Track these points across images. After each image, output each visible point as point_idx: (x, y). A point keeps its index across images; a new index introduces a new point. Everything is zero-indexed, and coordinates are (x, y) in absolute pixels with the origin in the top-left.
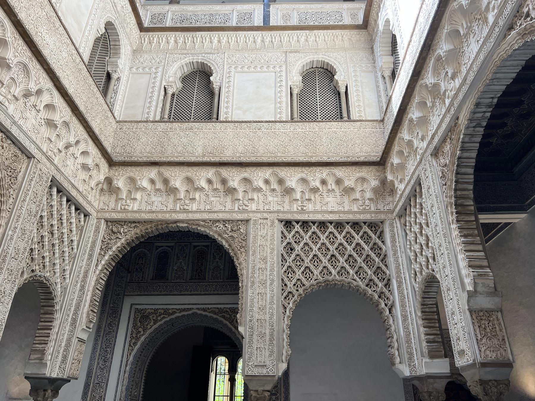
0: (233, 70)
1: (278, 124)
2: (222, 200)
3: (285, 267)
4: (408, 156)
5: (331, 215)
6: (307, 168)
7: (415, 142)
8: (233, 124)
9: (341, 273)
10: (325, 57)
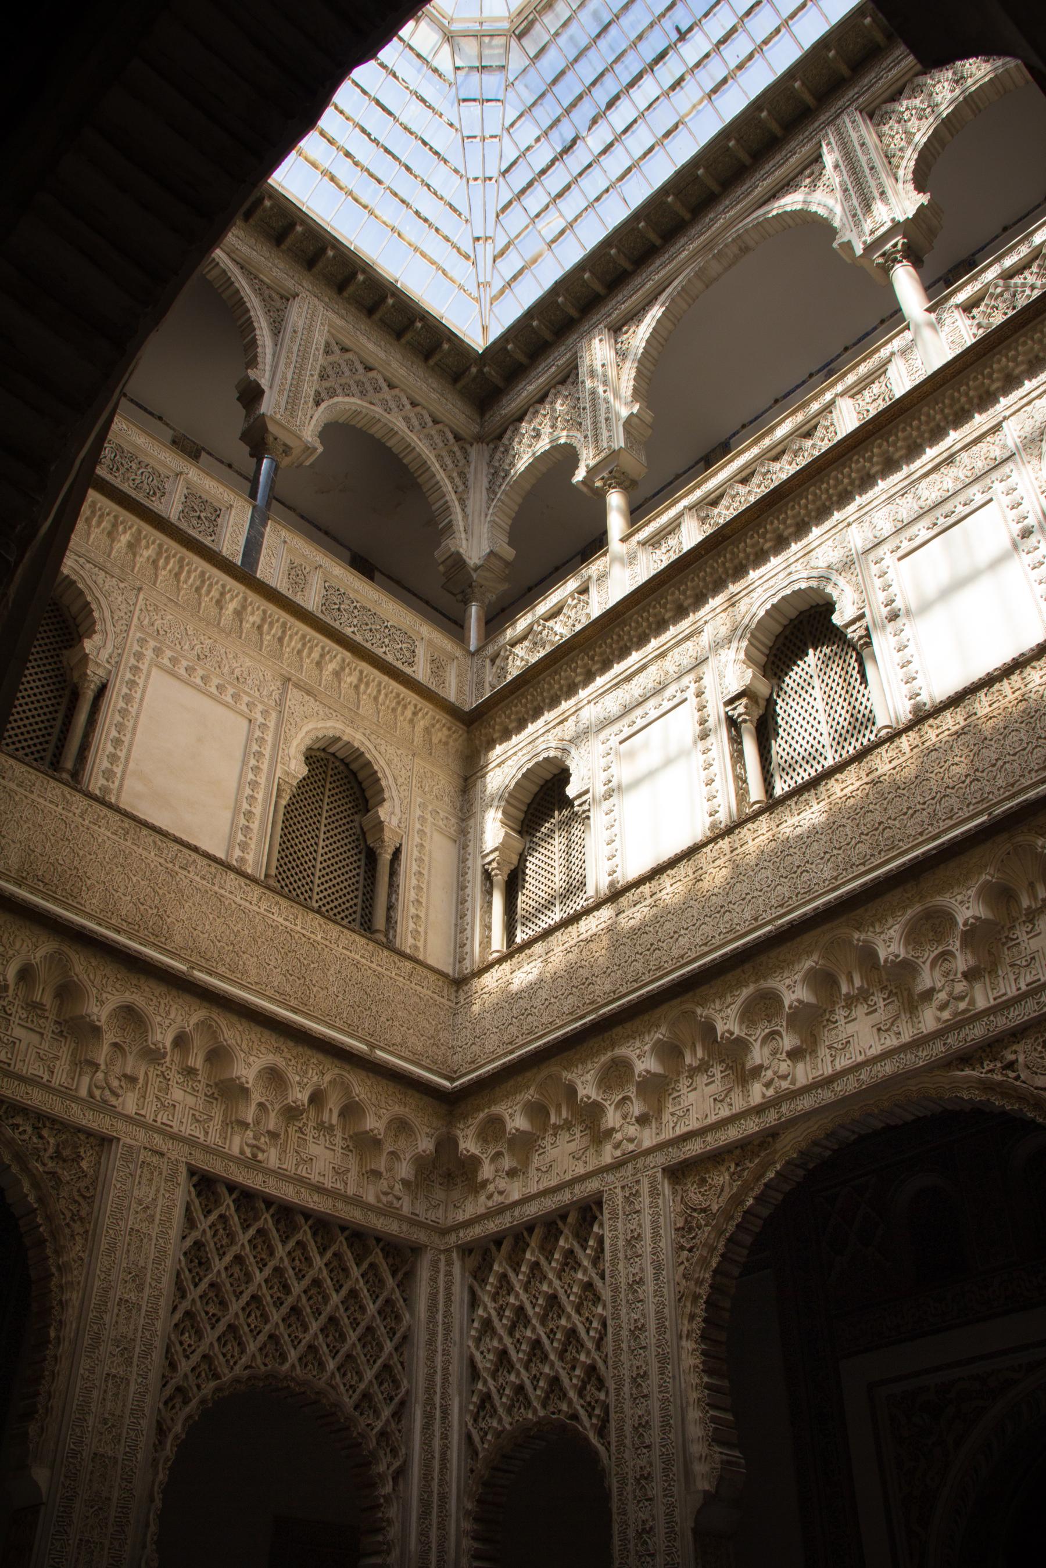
0: (149, 654)
1: (233, 876)
2: (45, 1045)
3: (178, 1315)
4: (556, 1127)
5: (316, 1198)
6: (291, 1044)
7: (610, 1111)
8: (117, 817)
9: (304, 1360)
10: (367, 743)
